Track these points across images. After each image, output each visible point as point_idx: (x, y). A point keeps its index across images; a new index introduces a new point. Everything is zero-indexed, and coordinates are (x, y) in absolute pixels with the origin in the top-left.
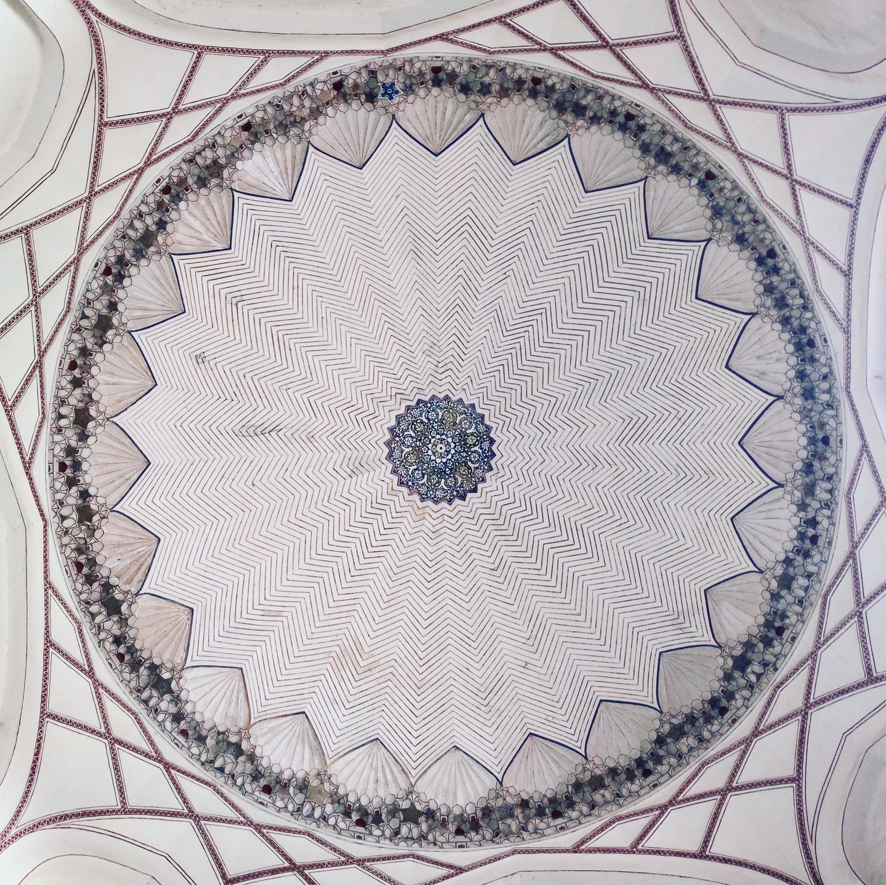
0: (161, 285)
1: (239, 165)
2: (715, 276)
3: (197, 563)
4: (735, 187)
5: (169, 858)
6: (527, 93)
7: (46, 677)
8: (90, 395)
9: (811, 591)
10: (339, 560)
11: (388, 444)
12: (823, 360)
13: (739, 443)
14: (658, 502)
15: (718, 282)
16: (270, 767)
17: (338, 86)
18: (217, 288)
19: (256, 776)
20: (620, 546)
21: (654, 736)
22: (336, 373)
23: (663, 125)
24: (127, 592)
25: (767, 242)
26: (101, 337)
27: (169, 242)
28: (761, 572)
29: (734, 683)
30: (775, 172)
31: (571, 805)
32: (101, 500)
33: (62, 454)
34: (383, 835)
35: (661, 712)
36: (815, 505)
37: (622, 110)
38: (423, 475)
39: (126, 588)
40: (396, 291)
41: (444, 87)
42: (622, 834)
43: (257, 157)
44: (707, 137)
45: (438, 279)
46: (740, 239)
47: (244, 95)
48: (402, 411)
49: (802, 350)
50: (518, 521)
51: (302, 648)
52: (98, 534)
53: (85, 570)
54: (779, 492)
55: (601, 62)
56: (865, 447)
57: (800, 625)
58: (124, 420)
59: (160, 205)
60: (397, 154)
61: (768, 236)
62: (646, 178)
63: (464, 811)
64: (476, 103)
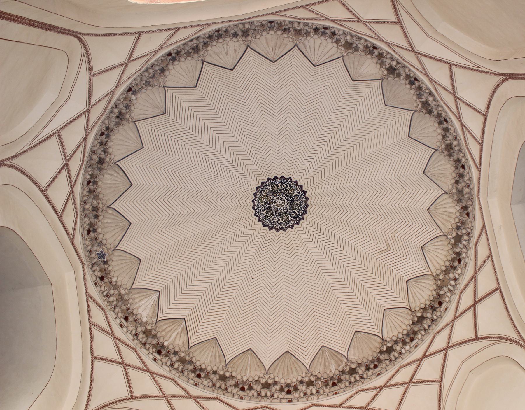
0: (203, 350)
2: (184, 79)
3: (335, 326)
4: (135, 79)
5: (463, 362)
8: (256, 381)
10: (335, 256)
11: (277, 230)
14: (306, 98)
15: (186, 77)
18: (204, 321)
19: (433, 309)
20: (329, 117)
22: (242, 258)
23: (105, 119)
25: (163, 59)
30: (124, 71)
32: (304, 375)
33: (283, 394)
38: (293, 212)
39: (344, 362)
40: (200, 232)
44: (109, 102)
45: (193, 211)
48: (261, 223)
49: (221, 35)
50: (317, 166)
51: (377, 277)
52: (319, 376)
53: (336, 381)
60: (132, 242)
61: (160, 59)
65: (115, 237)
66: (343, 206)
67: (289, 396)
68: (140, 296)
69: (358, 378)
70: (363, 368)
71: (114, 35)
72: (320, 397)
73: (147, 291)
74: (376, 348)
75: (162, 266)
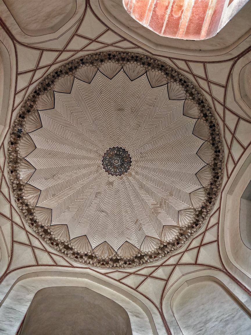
0: (42, 212)
1: (21, 178)
4: (88, 55)
6: (37, 96)
7: (127, 285)
8: (62, 243)
9: (197, 89)
11: (109, 174)
12: (142, 56)
13: (152, 88)
16: (173, 240)
17: (12, 144)
21: (211, 145)
23: (63, 65)
24: (115, 255)
26: (49, 233)
28: (186, 99)
29: (209, 120)
31: (217, 173)
33: (73, 256)
34: (202, 221)
35: (207, 141)
36: (177, 77)
37: (54, 74)
40: (72, 153)
41: (26, 116)
42: (231, 166)
43: (21, 173)
44: (72, 56)
46: (102, 61)
47: (4, 169)
48: (102, 166)
51: (148, 219)
53: (105, 263)
54: (169, 84)
55: (39, 74)
56: (170, 58)
57: (203, 97)
59: (22, 203)
61: (105, 53)
62: (74, 77)
63: (206, 199)
64: (34, 110)
65: (31, 128)
66: (146, 176)
67: (76, 259)
68: (25, 166)
70: (123, 262)
71: (99, 19)
73: (31, 166)
74: (133, 254)
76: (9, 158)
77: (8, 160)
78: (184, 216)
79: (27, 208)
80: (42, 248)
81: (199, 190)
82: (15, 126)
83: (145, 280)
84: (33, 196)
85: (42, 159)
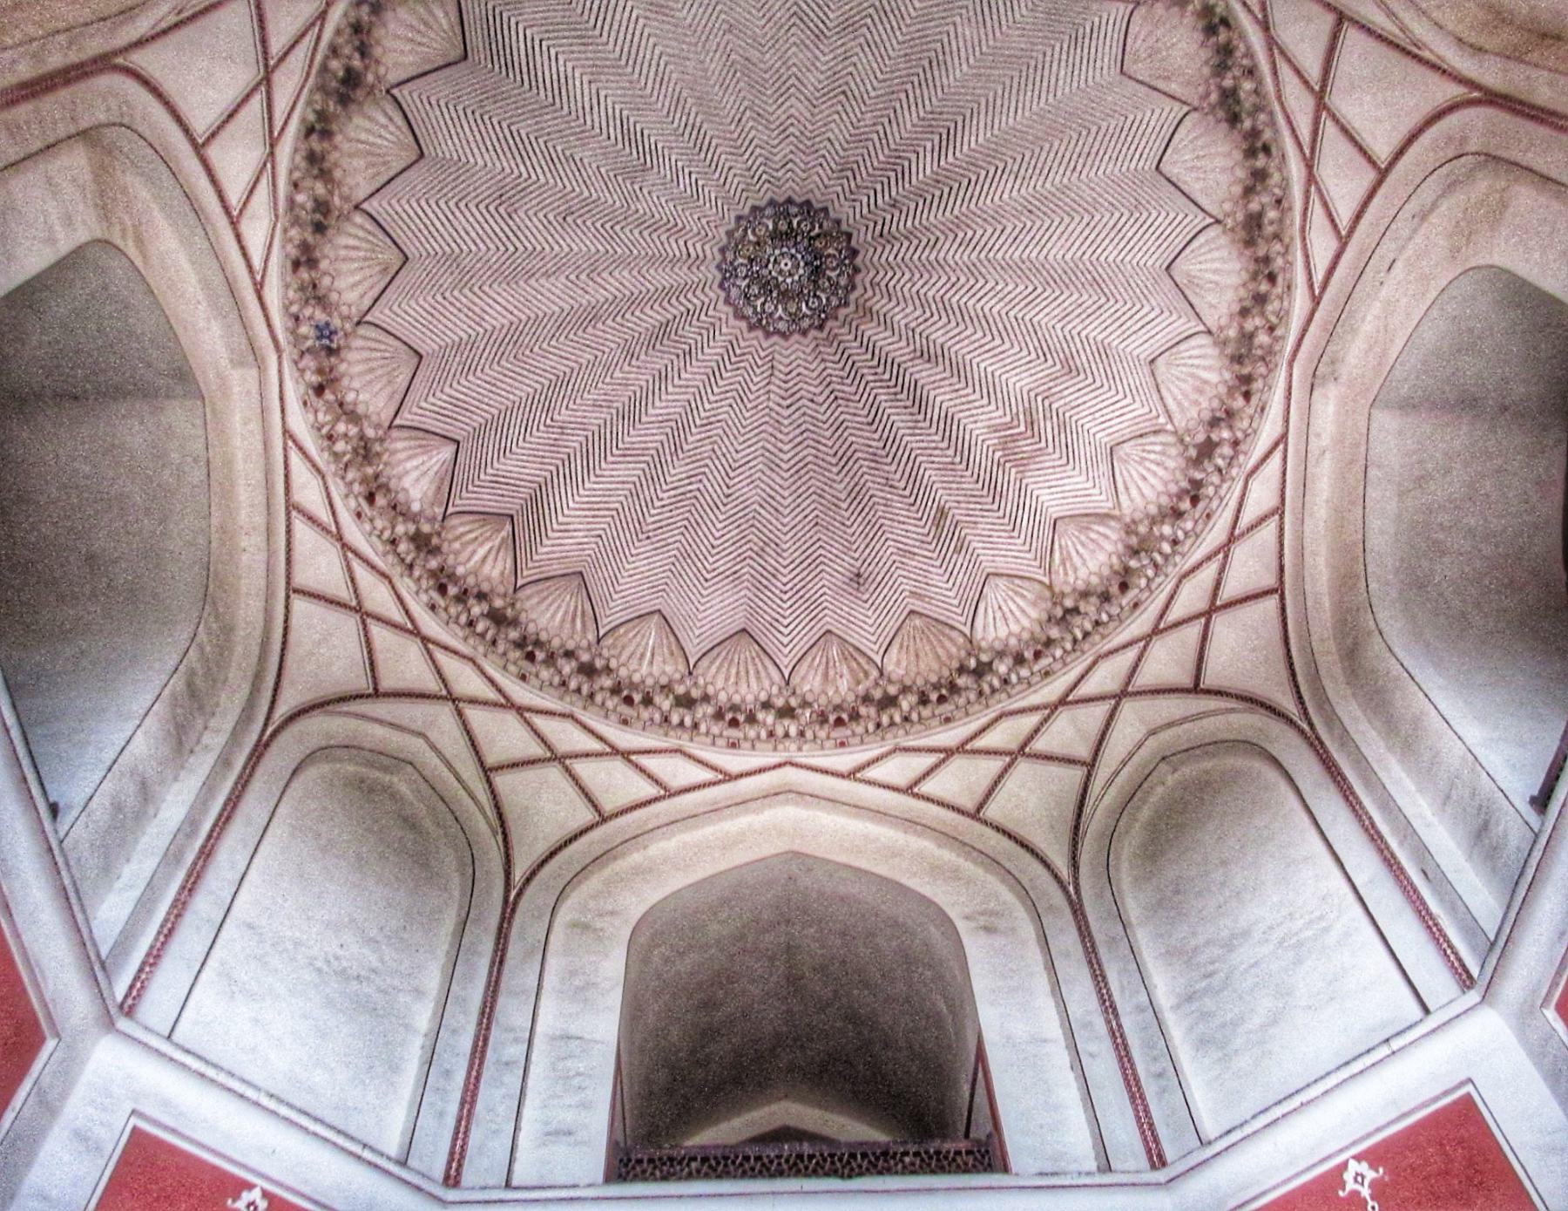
5: (1153, 733)
8: (663, 687)
11: (768, 335)
16: (1101, 577)
24: (877, 684)
27: (501, 590)
31: (1267, 260)
32: (775, 690)
33: (721, 723)
43: (407, 482)
52: (809, 698)
53: (845, 716)
58: (694, 650)
59: (462, 598)
67: (734, 733)
69: (897, 719)
70: (913, 699)
72: (805, 747)
74: (950, 657)
75: (470, 377)
76: (337, 456)
77: (333, 467)
78: (1140, 464)
79: (485, 607)
80: (596, 746)
81: (1193, 342)
82: (297, 319)
83: (1005, 770)
84: (487, 547)
85: (463, 381)
